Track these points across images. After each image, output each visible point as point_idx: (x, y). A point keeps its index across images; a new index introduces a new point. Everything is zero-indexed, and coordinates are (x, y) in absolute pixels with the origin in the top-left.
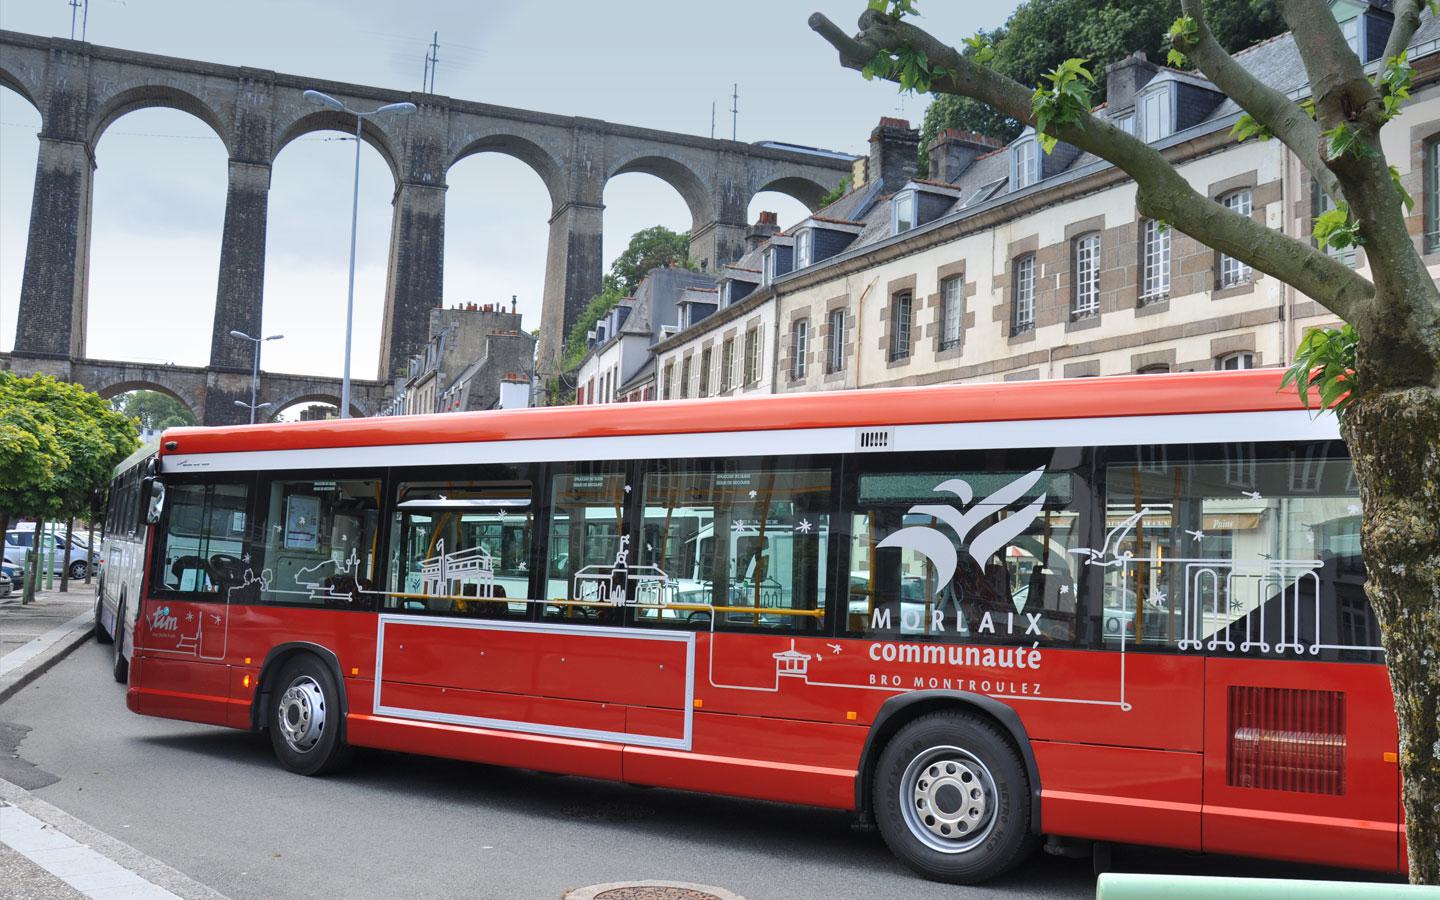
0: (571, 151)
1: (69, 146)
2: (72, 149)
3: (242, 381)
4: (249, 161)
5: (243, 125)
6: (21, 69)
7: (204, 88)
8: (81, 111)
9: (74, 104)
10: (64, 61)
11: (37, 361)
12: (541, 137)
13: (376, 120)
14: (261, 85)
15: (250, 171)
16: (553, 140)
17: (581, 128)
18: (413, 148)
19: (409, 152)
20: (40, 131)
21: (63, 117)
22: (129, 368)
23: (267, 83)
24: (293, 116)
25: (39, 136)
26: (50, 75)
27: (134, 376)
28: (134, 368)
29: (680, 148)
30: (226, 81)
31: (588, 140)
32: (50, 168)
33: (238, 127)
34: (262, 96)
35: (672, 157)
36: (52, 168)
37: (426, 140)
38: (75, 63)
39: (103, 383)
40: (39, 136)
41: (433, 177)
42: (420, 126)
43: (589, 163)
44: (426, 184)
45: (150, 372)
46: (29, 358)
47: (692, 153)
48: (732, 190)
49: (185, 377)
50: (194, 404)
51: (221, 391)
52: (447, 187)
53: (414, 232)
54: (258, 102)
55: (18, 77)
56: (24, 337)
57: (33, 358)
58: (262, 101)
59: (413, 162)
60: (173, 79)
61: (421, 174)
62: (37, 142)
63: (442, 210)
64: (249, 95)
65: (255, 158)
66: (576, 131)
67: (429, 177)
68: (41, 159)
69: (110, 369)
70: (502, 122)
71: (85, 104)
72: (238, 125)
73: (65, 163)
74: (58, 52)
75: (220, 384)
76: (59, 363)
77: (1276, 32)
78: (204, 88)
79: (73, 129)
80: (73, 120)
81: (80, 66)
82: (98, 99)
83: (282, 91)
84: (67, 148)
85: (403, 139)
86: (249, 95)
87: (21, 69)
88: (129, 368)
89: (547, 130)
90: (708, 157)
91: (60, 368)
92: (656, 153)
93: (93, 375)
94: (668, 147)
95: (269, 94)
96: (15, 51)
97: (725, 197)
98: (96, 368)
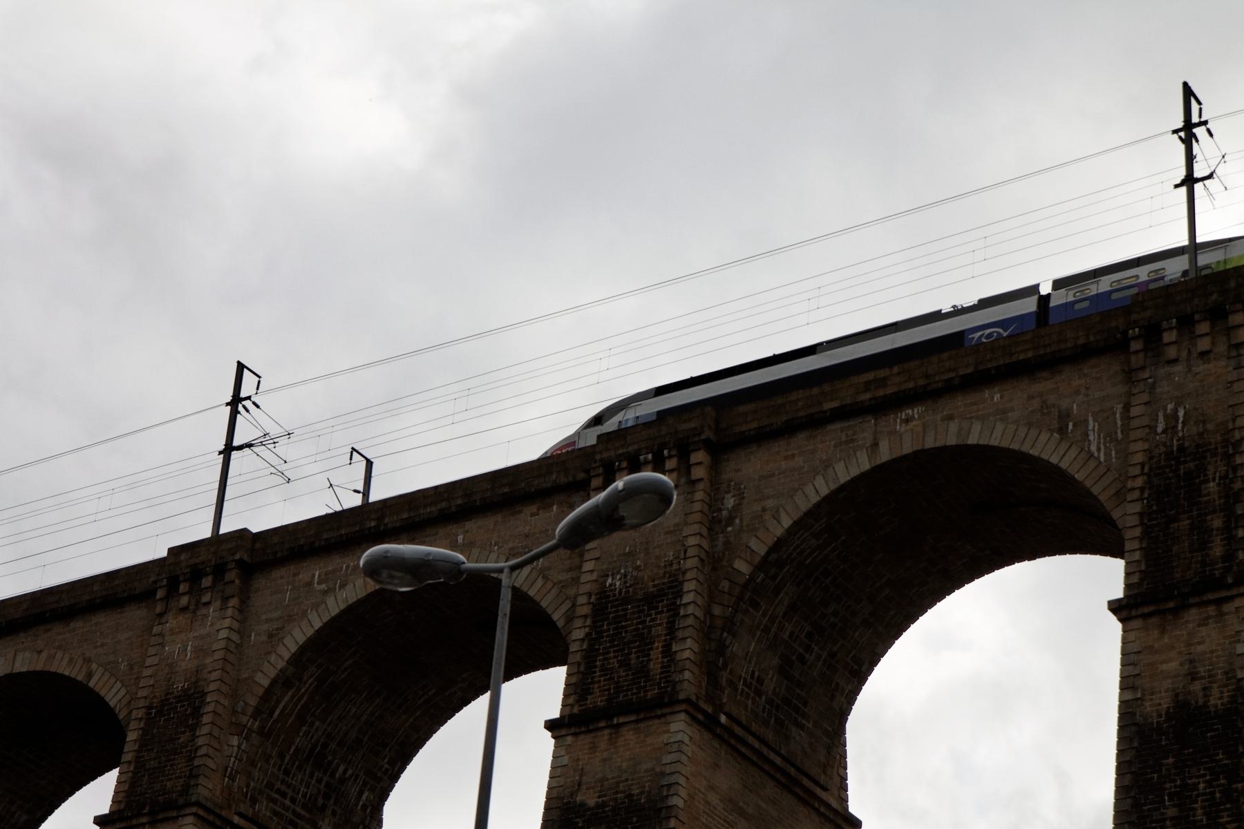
1: (1211, 610)
2: (1221, 615)
6: (1062, 430)
9: (1215, 468)
10: (1172, 352)
20: (1119, 594)
25: (1116, 607)
26: (1135, 411)
32: (1159, 702)
36: (1165, 702)
38: (1204, 344)
40: (1116, 607)
55: (1054, 460)
62: (1114, 628)
68: (1127, 683)
73: (1202, 670)
74: (1152, 334)
79: (1217, 550)
80: (1217, 523)
81: (1221, 348)
84: (1204, 622)
87: (1062, 430)
96: (1044, 386)
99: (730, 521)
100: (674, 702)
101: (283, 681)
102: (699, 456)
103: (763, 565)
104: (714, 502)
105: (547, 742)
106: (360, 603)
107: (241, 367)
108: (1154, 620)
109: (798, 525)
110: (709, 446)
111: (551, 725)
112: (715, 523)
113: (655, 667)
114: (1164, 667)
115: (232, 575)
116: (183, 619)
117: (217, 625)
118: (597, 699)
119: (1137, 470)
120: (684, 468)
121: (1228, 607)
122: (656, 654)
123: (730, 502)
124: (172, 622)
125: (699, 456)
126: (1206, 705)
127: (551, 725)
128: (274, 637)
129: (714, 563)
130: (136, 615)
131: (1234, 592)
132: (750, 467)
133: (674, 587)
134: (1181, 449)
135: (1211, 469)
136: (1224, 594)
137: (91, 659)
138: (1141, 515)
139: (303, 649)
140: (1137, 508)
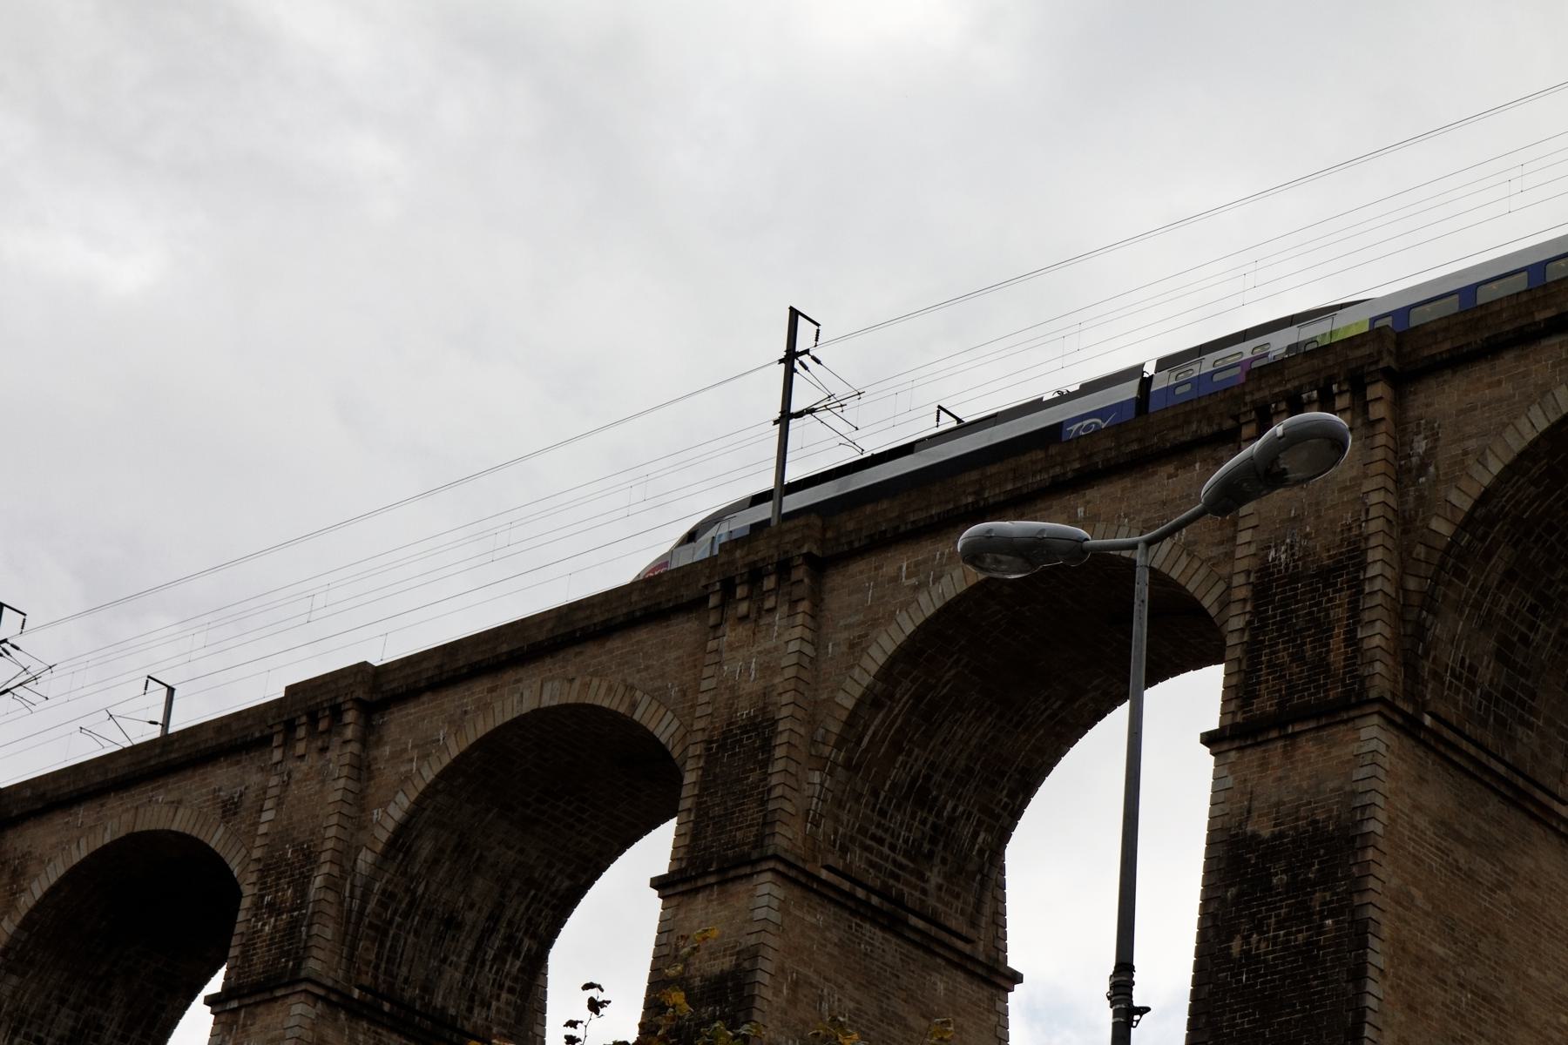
99: (1423, 468)
100: (1364, 702)
101: (872, 701)
102: (1377, 390)
103: (1468, 523)
104: (1400, 448)
105: (1205, 760)
106: (960, 598)
107: (794, 314)
109: (1510, 470)
110: (1388, 375)
111: (1209, 739)
112: (1403, 473)
113: (1337, 658)
115: (799, 573)
116: (742, 631)
117: (785, 635)
118: (1265, 704)
120: (1360, 406)
122: (1337, 642)
123: (1421, 445)
124: (730, 634)
125: (1377, 390)
127: (1209, 739)
128: (857, 646)
129: (1405, 524)
130: (685, 629)
132: (1443, 399)
133: (1353, 558)
137: (633, 686)
139: (893, 660)
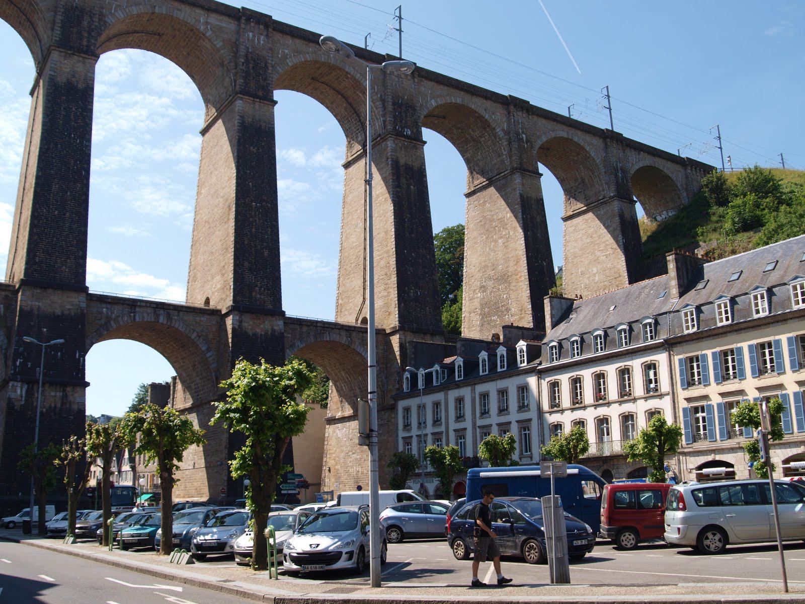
0: (509, 125)
1: (81, 59)
3: (266, 322)
4: (255, 96)
5: (247, 61)
7: (207, 23)
8: (93, 27)
11: (50, 291)
12: (485, 110)
13: (358, 75)
14: (262, 27)
15: (257, 107)
16: (493, 114)
17: (515, 106)
18: (394, 104)
19: (390, 107)
21: (75, 30)
22: (140, 306)
23: (267, 26)
24: (288, 61)
27: (145, 315)
28: (146, 306)
29: (579, 133)
30: (226, 19)
31: (520, 116)
33: (243, 63)
34: (262, 37)
35: (576, 139)
36: (64, 80)
37: (403, 99)
39: (112, 323)
41: (412, 132)
42: (396, 85)
43: (524, 136)
44: (407, 137)
45: (162, 312)
46: (41, 288)
47: (588, 138)
48: (620, 172)
49: (198, 318)
50: (208, 350)
51: (246, 332)
52: (425, 143)
53: (403, 181)
54: (259, 42)
56: (35, 263)
57: (45, 288)
58: (262, 42)
59: (395, 117)
60: (178, 10)
61: (403, 128)
63: (423, 164)
64: (251, 34)
65: (260, 94)
66: (512, 107)
67: (409, 133)
69: (120, 307)
70: (457, 92)
71: (97, 20)
72: (243, 61)
73: (77, 76)
75: (245, 324)
76: (73, 295)
77: (578, 199)
78: (207, 23)
82: (106, 19)
83: (277, 36)
84: (79, 61)
85: (381, 96)
86: (251, 34)
88: (140, 306)
89: (489, 104)
90: (597, 142)
91: (76, 301)
92: (565, 135)
93: (101, 313)
94: (572, 131)
95: (267, 36)
97: (616, 176)
98: (104, 305)
108: (63, 54)
114: (64, 69)
119: (61, 7)
121: (87, 61)
126: (77, 86)
131: (89, 57)
134: (76, 7)
135: (85, 18)
136: (87, 56)
138: (62, 20)
140: (60, 17)
